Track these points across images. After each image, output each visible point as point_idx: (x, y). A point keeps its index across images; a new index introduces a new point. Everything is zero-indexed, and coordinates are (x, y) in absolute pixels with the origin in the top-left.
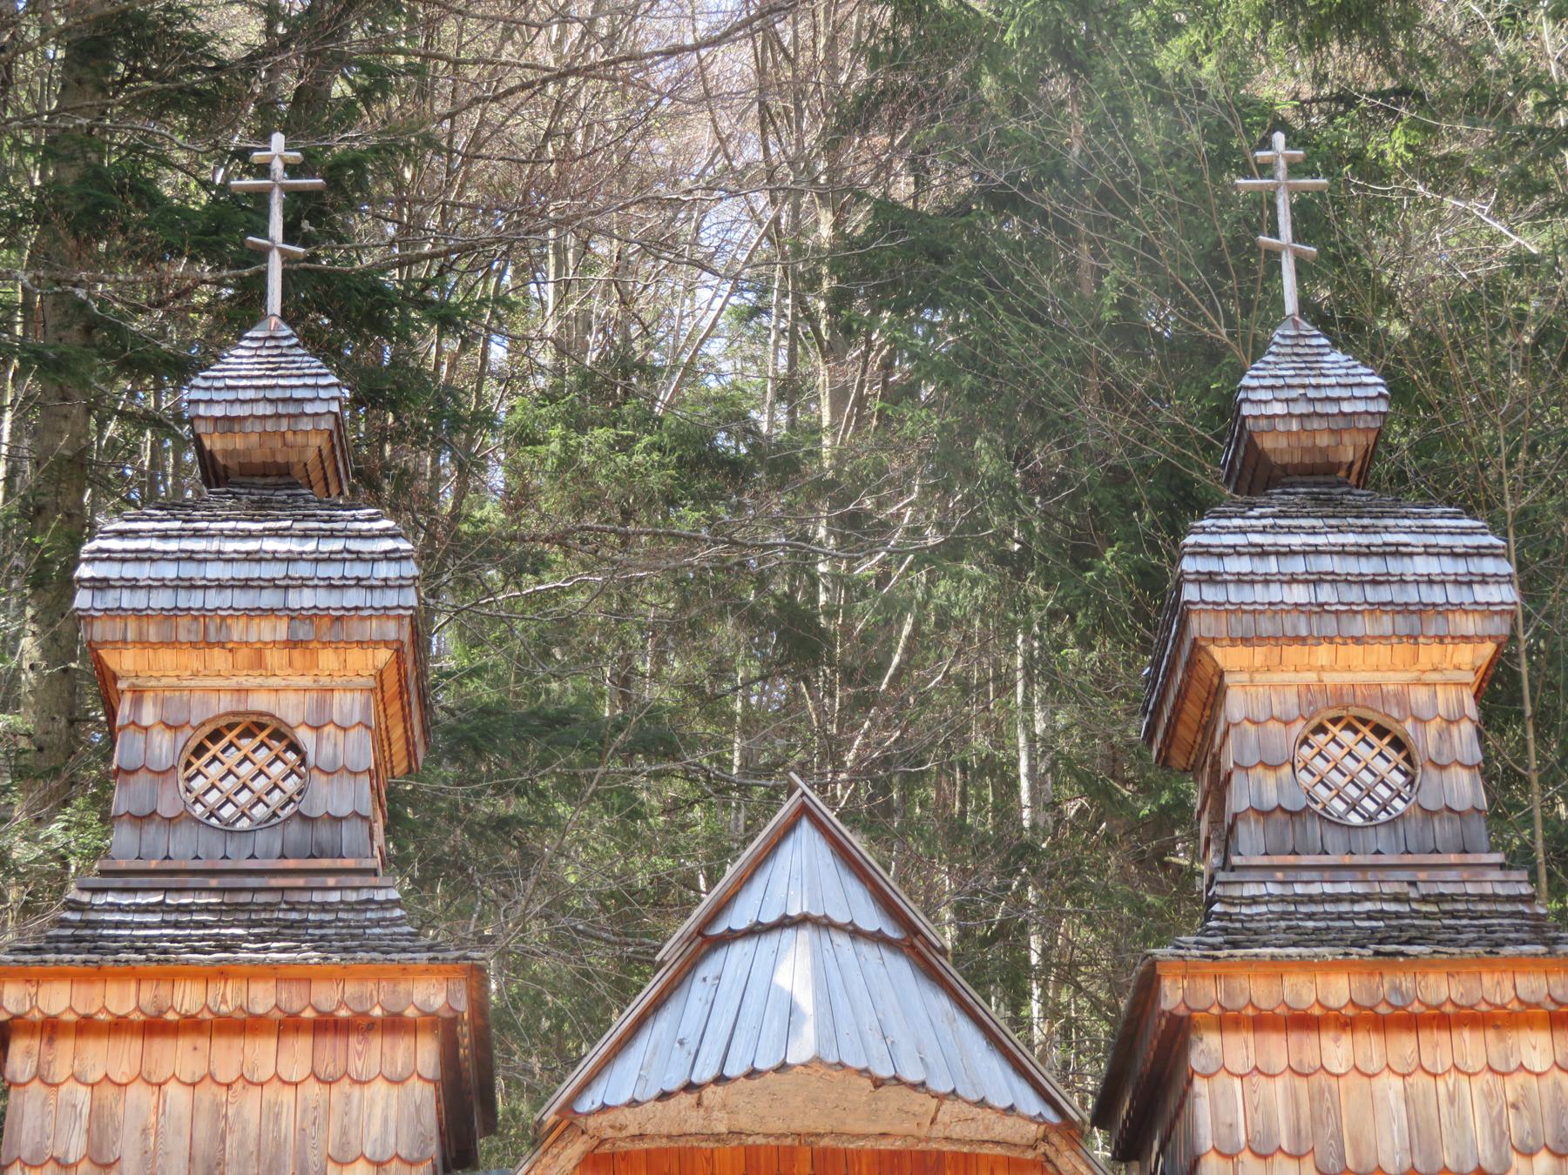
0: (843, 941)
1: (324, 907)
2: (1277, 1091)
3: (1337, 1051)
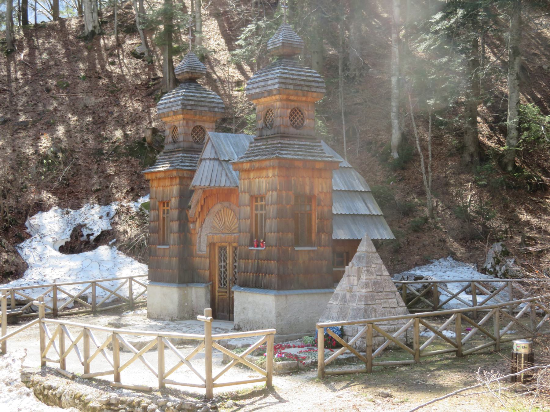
0: (208, 161)
1: (176, 157)
2: (246, 181)
3: (252, 175)
